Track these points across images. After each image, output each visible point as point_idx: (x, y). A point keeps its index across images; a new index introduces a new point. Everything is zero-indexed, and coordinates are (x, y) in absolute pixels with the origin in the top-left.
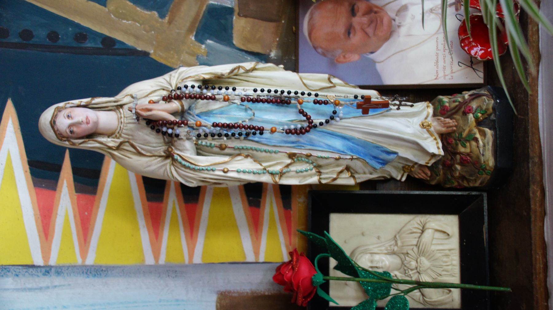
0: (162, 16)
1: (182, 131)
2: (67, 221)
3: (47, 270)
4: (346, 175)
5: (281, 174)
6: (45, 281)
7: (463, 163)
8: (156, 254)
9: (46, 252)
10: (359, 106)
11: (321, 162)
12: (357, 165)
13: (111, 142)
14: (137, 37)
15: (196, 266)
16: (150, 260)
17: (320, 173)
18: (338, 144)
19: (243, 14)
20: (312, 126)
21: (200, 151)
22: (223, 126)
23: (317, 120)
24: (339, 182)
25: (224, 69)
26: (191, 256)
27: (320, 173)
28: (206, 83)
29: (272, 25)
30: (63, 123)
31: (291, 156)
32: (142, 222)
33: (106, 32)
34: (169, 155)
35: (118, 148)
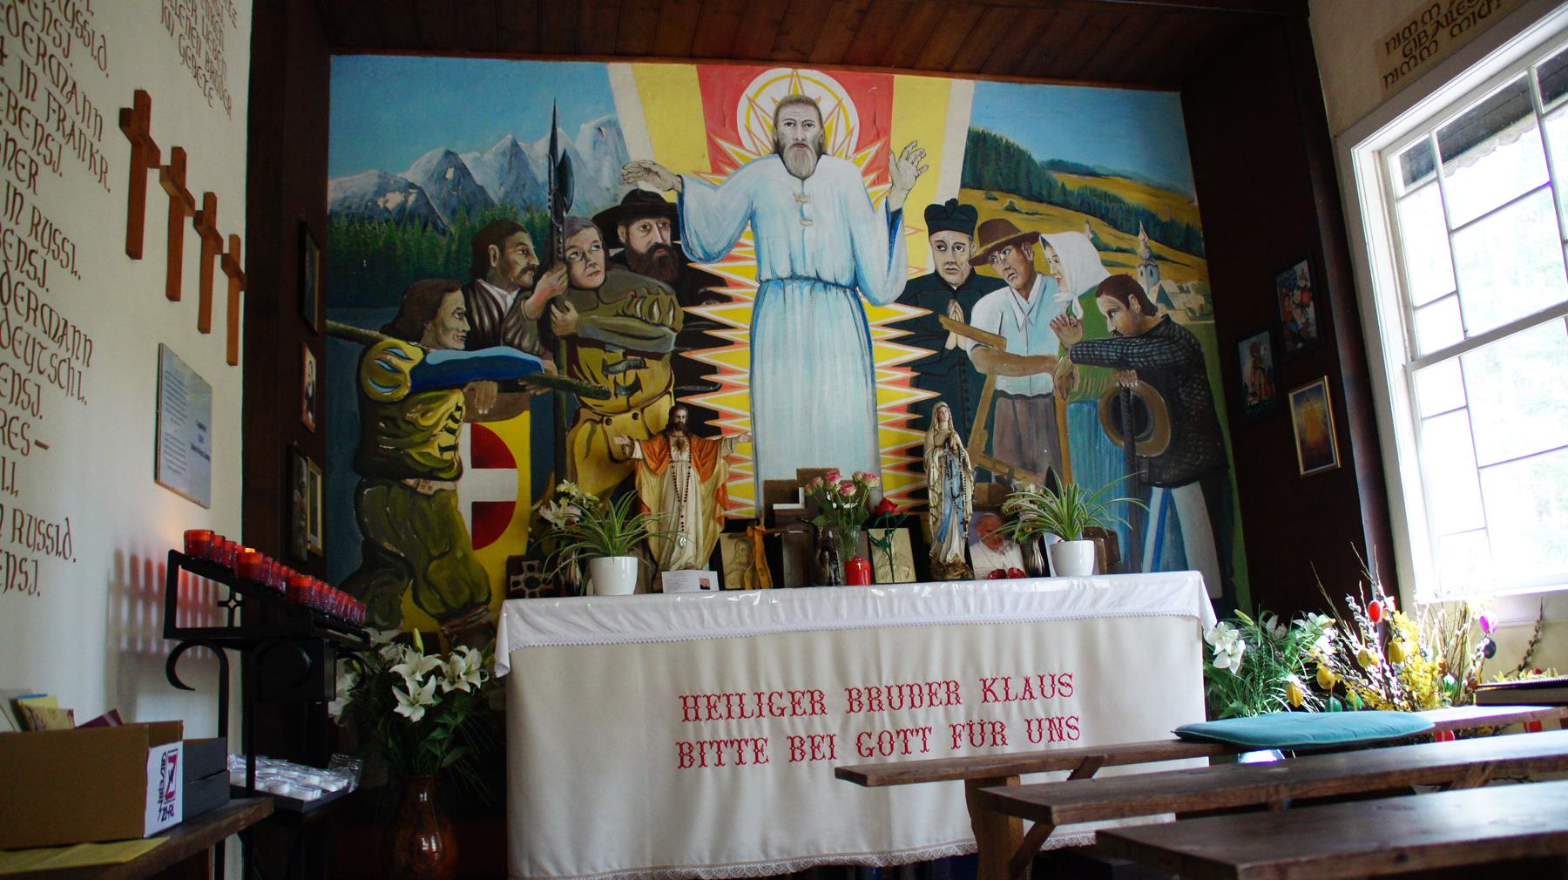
0: (984, 452)
1: (947, 450)
2: (893, 417)
3: (875, 411)
4: (934, 520)
5: (933, 490)
6: (871, 411)
7: (945, 570)
8: (884, 453)
9: (881, 410)
10: (963, 520)
11: (939, 508)
12: (939, 524)
13: (937, 427)
14: (973, 442)
15: (880, 470)
16: (881, 451)
17: (934, 507)
18: (947, 512)
19: (989, 486)
20: (954, 498)
21: (939, 458)
22: (951, 465)
23: (957, 500)
24: (931, 517)
25: (970, 467)
26: (884, 468)
27: (934, 507)
28: (964, 460)
29: (986, 500)
30: (944, 409)
31: (941, 494)
32: (897, 447)
33: (973, 430)
34: (936, 447)
35: (935, 430)
